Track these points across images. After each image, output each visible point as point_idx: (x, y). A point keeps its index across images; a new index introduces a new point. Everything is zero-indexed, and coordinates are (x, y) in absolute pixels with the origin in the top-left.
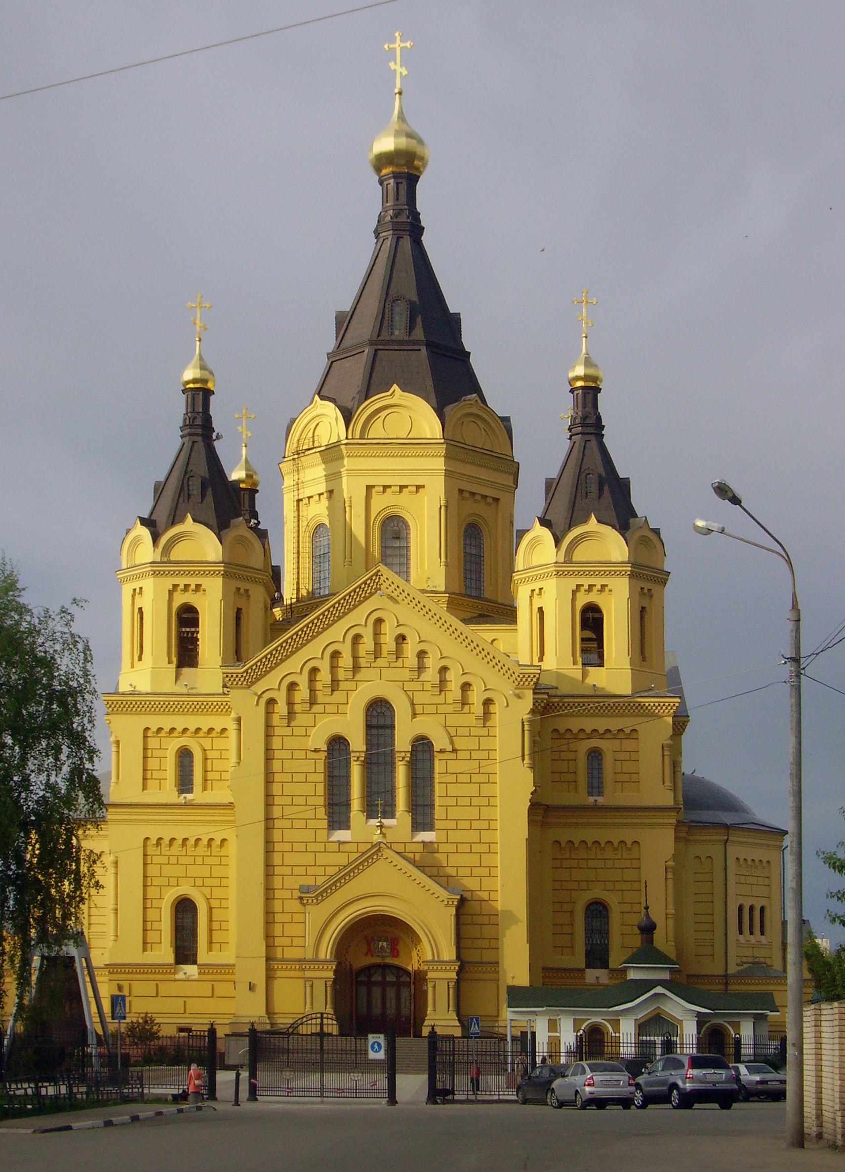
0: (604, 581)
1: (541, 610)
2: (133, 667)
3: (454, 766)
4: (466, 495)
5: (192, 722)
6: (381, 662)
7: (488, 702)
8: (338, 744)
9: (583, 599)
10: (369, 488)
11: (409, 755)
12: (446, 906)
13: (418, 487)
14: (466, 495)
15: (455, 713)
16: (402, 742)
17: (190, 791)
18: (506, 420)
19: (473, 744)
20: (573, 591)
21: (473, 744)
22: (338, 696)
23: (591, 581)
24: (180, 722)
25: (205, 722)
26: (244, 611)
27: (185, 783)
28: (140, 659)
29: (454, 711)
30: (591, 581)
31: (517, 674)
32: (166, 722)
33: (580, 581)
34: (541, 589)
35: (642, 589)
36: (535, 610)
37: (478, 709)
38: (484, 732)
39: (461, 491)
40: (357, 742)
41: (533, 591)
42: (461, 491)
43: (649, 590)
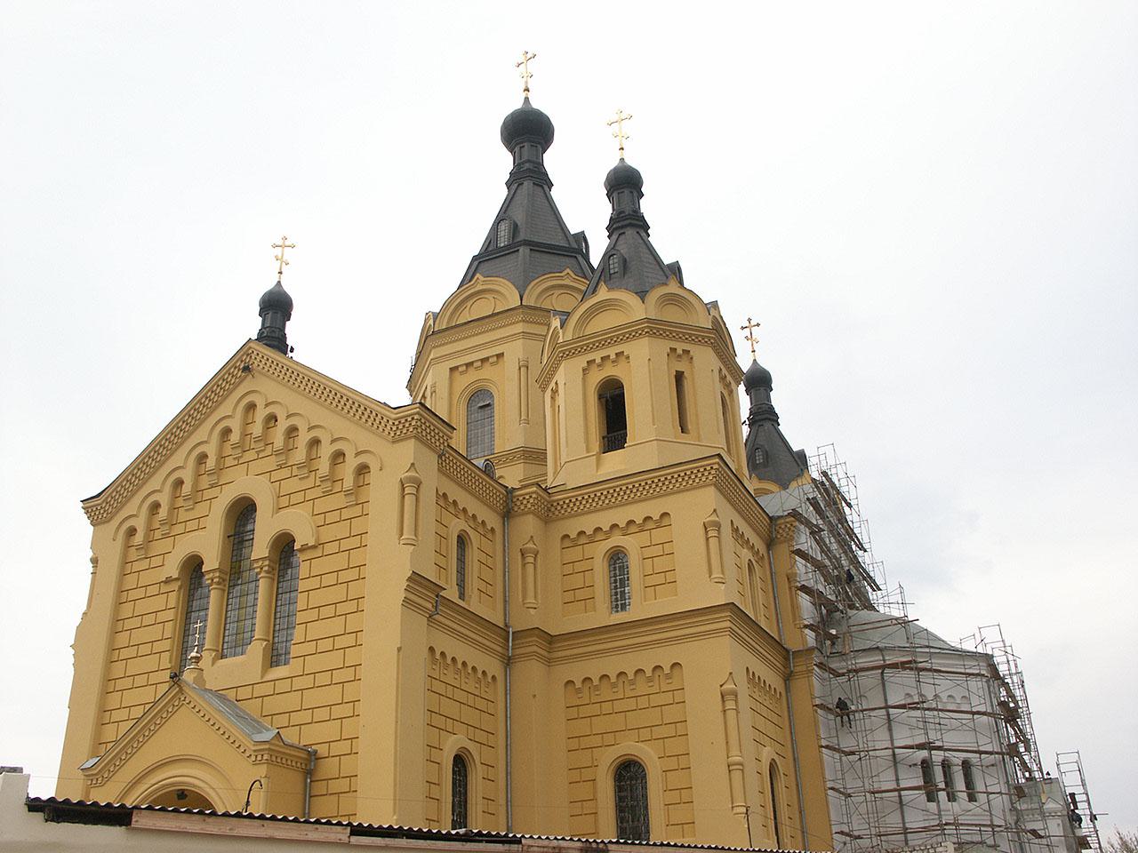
0: (618, 349)
3: (319, 566)
6: (250, 455)
7: (363, 470)
8: (193, 567)
9: (597, 377)
11: (267, 563)
12: (255, 763)
15: (327, 493)
16: (260, 548)
19: (340, 530)
20: (584, 370)
21: (340, 530)
22: (201, 509)
23: (604, 353)
29: (323, 492)
30: (604, 353)
31: (391, 423)
33: (590, 357)
35: (673, 350)
37: (349, 482)
38: (357, 510)
40: (211, 562)
43: (686, 352)
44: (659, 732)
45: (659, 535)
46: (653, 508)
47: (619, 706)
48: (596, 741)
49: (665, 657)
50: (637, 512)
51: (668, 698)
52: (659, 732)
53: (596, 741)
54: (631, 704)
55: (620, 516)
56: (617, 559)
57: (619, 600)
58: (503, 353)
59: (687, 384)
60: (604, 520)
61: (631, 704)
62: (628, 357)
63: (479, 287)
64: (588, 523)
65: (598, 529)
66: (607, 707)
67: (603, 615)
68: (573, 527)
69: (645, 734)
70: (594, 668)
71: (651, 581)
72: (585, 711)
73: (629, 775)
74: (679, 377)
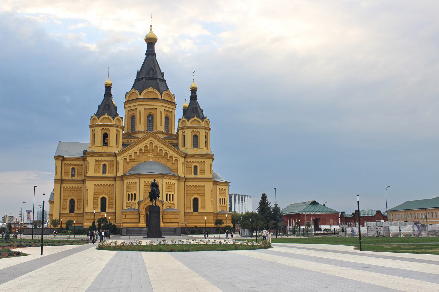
1: (184, 136)
2: (92, 146)
4: (166, 110)
5: (106, 158)
10: (144, 108)
13: (155, 108)
14: (166, 110)
17: (105, 174)
18: (174, 95)
20: (192, 132)
24: (103, 158)
25: (109, 158)
26: (118, 134)
27: (104, 172)
28: (94, 144)
32: (100, 158)
34: (184, 131)
35: (206, 132)
36: (183, 136)
39: (165, 110)
41: (183, 132)
42: (165, 110)
44: (200, 194)
45: (203, 164)
46: (203, 160)
47: (195, 190)
48: (191, 194)
49: (203, 184)
50: (200, 160)
51: (202, 190)
52: (200, 194)
53: (191, 194)
54: (197, 190)
55: (197, 160)
56: (196, 167)
57: (196, 173)
58: (157, 109)
59: (207, 138)
60: (194, 160)
61: (197, 190)
62: (199, 132)
63: (151, 90)
64: (191, 160)
65: (193, 161)
66: (193, 190)
67: (193, 176)
68: (189, 160)
69: (199, 194)
70: (191, 184)
71: (201, 172)
73: (196, 201)
74: (206, 136)
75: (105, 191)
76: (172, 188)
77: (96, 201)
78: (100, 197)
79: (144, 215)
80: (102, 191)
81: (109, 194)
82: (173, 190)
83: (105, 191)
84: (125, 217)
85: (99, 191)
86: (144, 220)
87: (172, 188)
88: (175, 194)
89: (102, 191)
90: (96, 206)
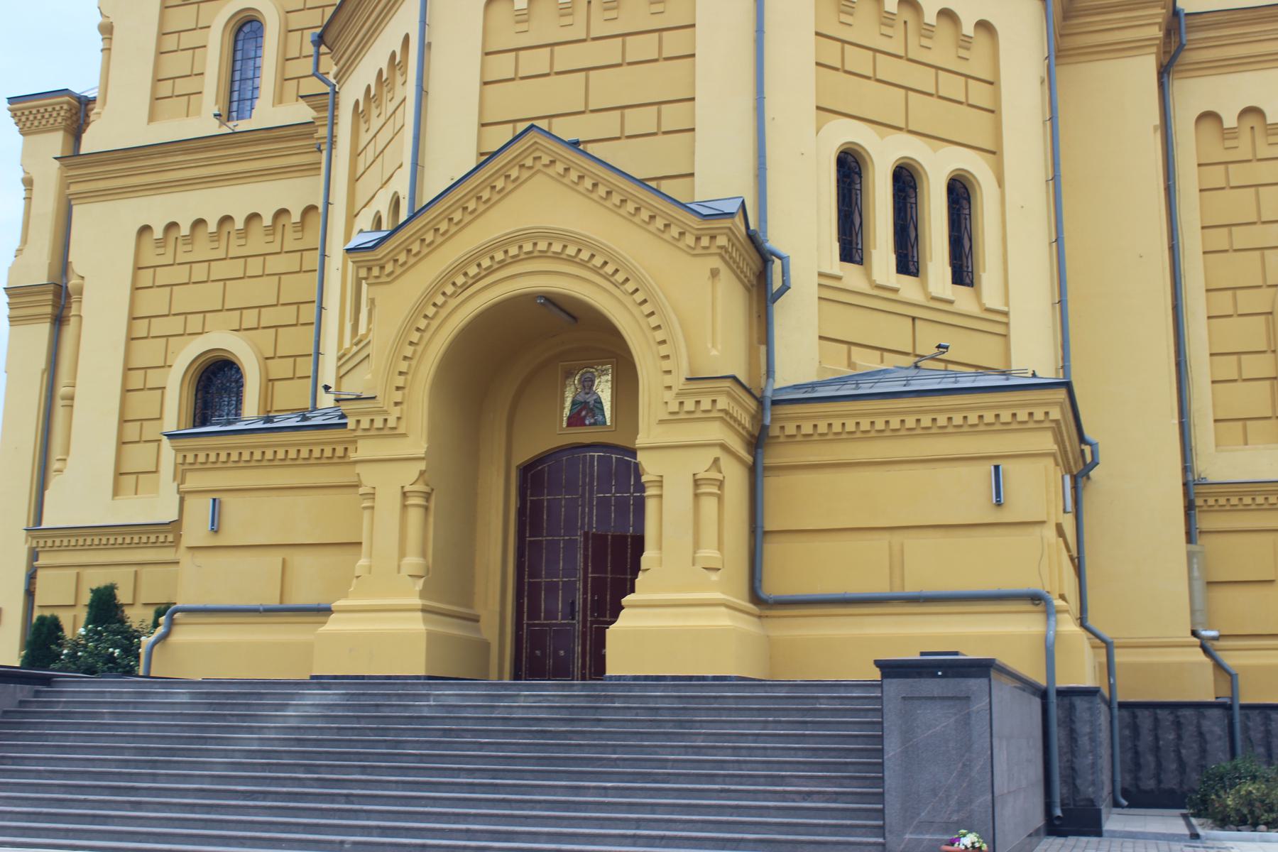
72: (1239, 175)
75: (239, 294)
76: (953, 87)
77: (142, 405)
78: (188, 353)
79: (409, 475)
80: (209, 296)
81: (269, 317)
82: (975, 126)
83: (239, 294)
84: (215, 528)
85: (186, 299)
86: (413, 561)
87: (953, 87)
88: (1000, 182)
89: (209, 296)
90: (139, 457)
